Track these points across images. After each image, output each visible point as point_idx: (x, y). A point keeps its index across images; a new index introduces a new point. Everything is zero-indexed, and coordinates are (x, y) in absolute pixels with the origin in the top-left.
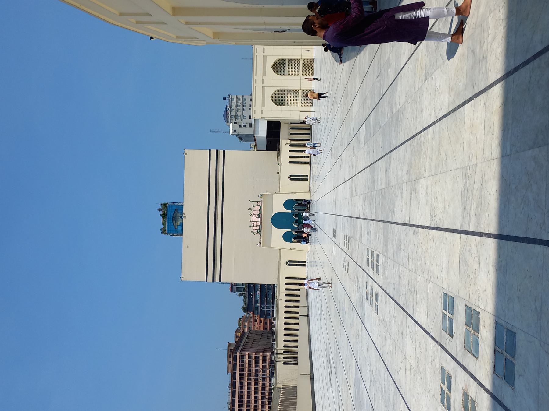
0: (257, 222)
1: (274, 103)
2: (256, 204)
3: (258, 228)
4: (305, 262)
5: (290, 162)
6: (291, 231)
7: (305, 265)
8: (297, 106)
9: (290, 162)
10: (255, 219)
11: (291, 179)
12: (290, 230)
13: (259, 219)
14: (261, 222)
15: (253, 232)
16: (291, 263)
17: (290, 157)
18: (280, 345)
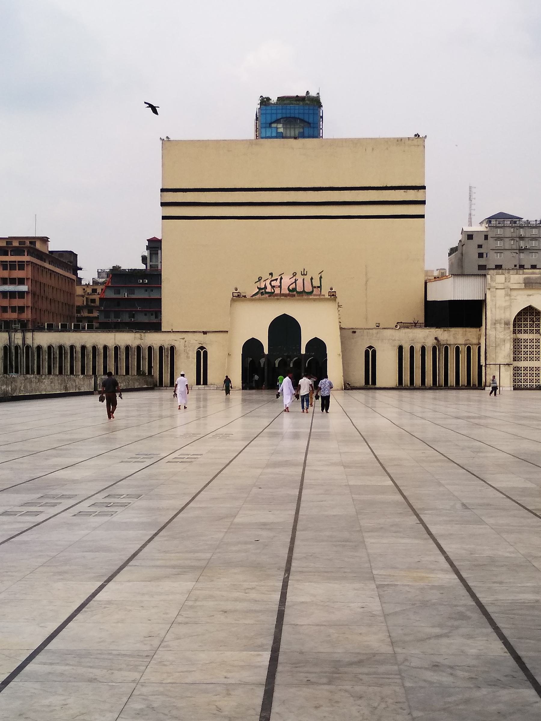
0: (280, 287)
1: (519, 314)
2: (316, 283)
3: (269, 289)
4: (205, 383)
5: (401, 348)
6: (263, 355)
7: (198, 383)
8: (514, 360)
9: (401, 348)
10: (287, 282)
11: (367, 352)
12: (266, 351)
13: (285, 291)
14: (281, 295)
15: (260, 279)
16: (202, 356)
17: (412, 348)
18: (43, 339)
